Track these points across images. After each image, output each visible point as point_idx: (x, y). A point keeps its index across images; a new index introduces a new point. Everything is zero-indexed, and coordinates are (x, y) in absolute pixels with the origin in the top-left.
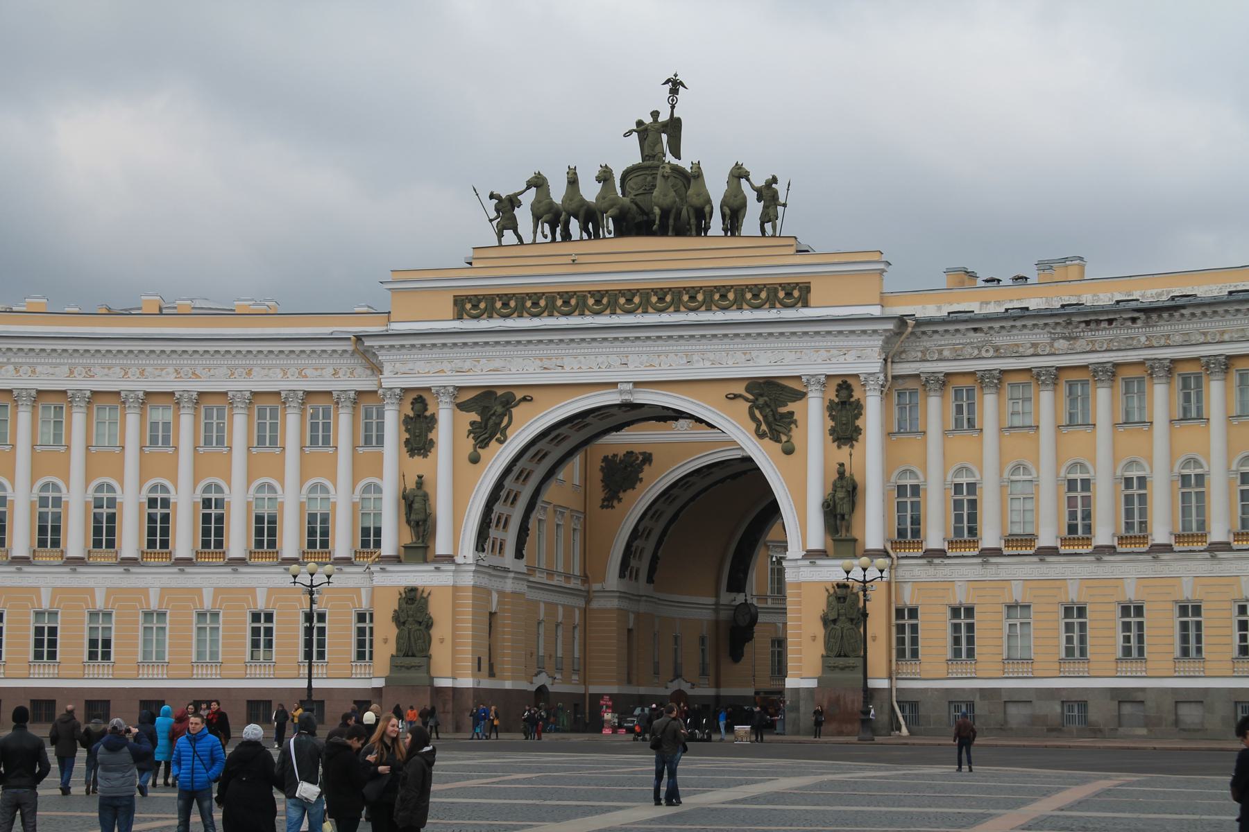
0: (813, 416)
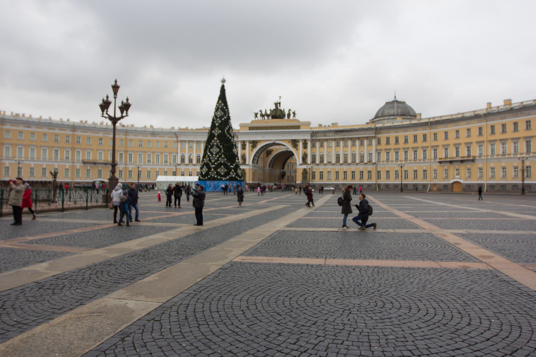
0: (301, 145)
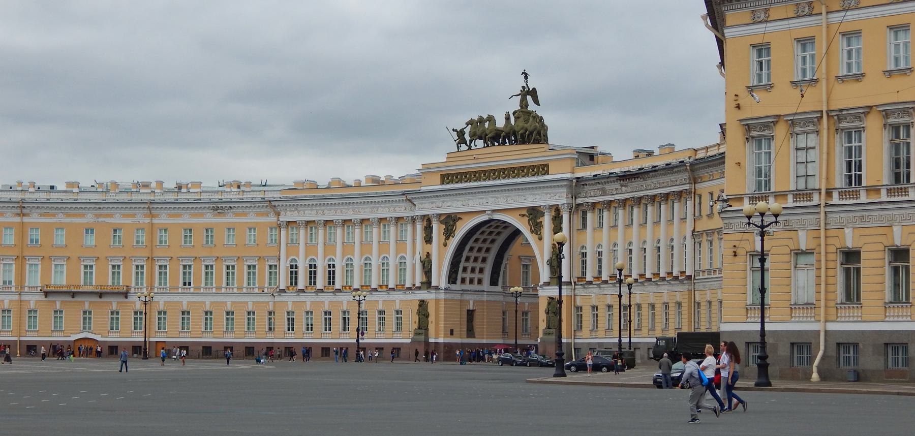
0: (547, 221)
